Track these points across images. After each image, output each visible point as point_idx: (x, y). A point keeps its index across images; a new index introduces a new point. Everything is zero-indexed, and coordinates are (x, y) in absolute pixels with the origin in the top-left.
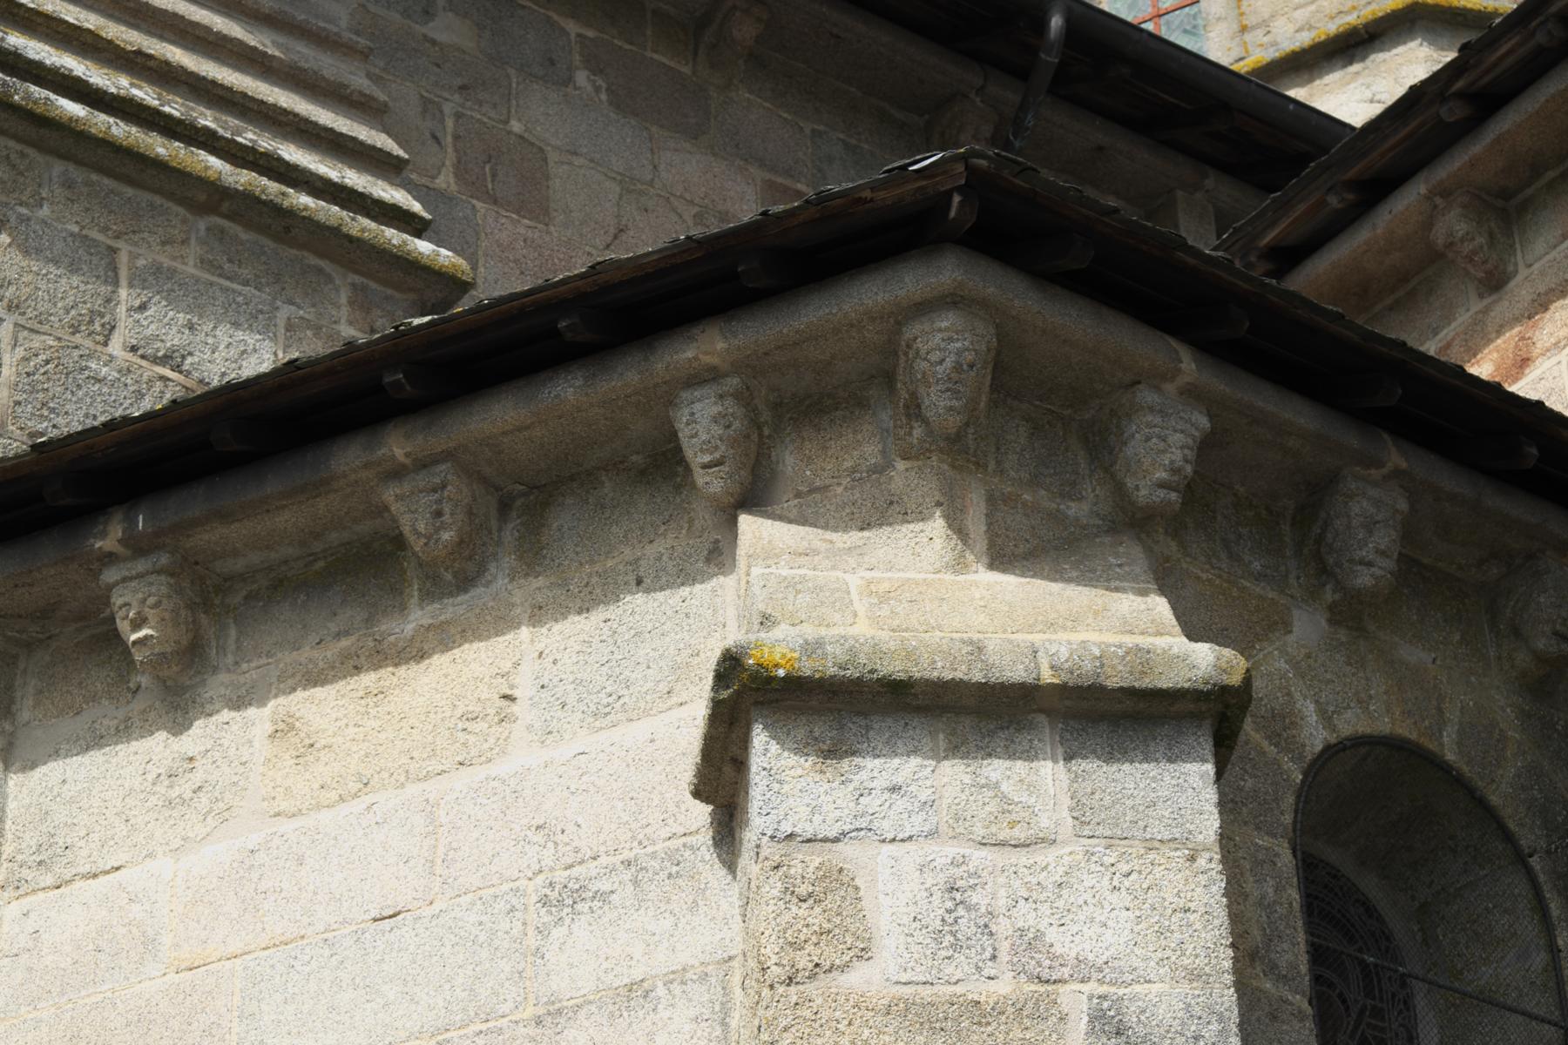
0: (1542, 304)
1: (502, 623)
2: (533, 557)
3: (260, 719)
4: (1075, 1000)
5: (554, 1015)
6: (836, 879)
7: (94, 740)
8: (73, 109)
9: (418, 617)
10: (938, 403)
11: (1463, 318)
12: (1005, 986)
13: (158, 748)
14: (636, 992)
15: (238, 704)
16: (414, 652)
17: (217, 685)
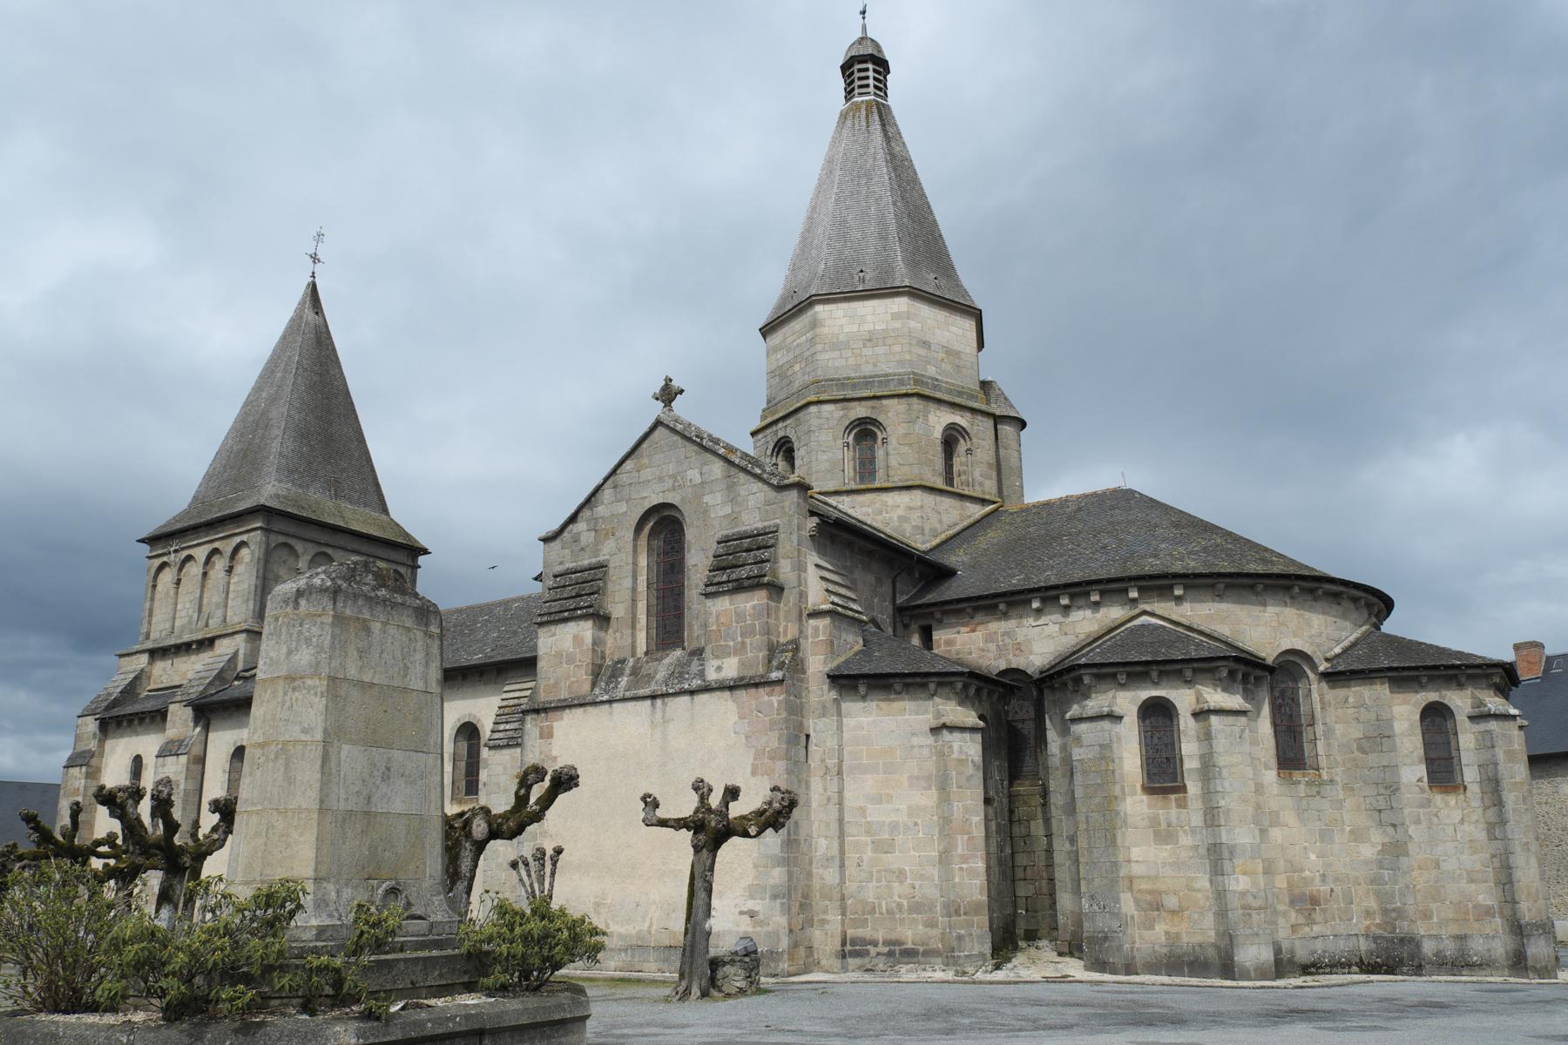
0: (979, 624)
1: (904, 700)
2: (907, 693)
3: (875, 703)
4: (970, 759)
5: (912, 747)
6: (951, 747)
7: (853, 701)
8: (840, 609)
9: (893, 696)
10: (958, 691)
11: (965, 620)
12: (964, 757)
13: (860, 705)
14: (922, 746)
15: (872, 701)
16: (893, 700)
17: (868, 698)
